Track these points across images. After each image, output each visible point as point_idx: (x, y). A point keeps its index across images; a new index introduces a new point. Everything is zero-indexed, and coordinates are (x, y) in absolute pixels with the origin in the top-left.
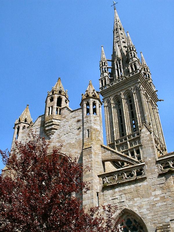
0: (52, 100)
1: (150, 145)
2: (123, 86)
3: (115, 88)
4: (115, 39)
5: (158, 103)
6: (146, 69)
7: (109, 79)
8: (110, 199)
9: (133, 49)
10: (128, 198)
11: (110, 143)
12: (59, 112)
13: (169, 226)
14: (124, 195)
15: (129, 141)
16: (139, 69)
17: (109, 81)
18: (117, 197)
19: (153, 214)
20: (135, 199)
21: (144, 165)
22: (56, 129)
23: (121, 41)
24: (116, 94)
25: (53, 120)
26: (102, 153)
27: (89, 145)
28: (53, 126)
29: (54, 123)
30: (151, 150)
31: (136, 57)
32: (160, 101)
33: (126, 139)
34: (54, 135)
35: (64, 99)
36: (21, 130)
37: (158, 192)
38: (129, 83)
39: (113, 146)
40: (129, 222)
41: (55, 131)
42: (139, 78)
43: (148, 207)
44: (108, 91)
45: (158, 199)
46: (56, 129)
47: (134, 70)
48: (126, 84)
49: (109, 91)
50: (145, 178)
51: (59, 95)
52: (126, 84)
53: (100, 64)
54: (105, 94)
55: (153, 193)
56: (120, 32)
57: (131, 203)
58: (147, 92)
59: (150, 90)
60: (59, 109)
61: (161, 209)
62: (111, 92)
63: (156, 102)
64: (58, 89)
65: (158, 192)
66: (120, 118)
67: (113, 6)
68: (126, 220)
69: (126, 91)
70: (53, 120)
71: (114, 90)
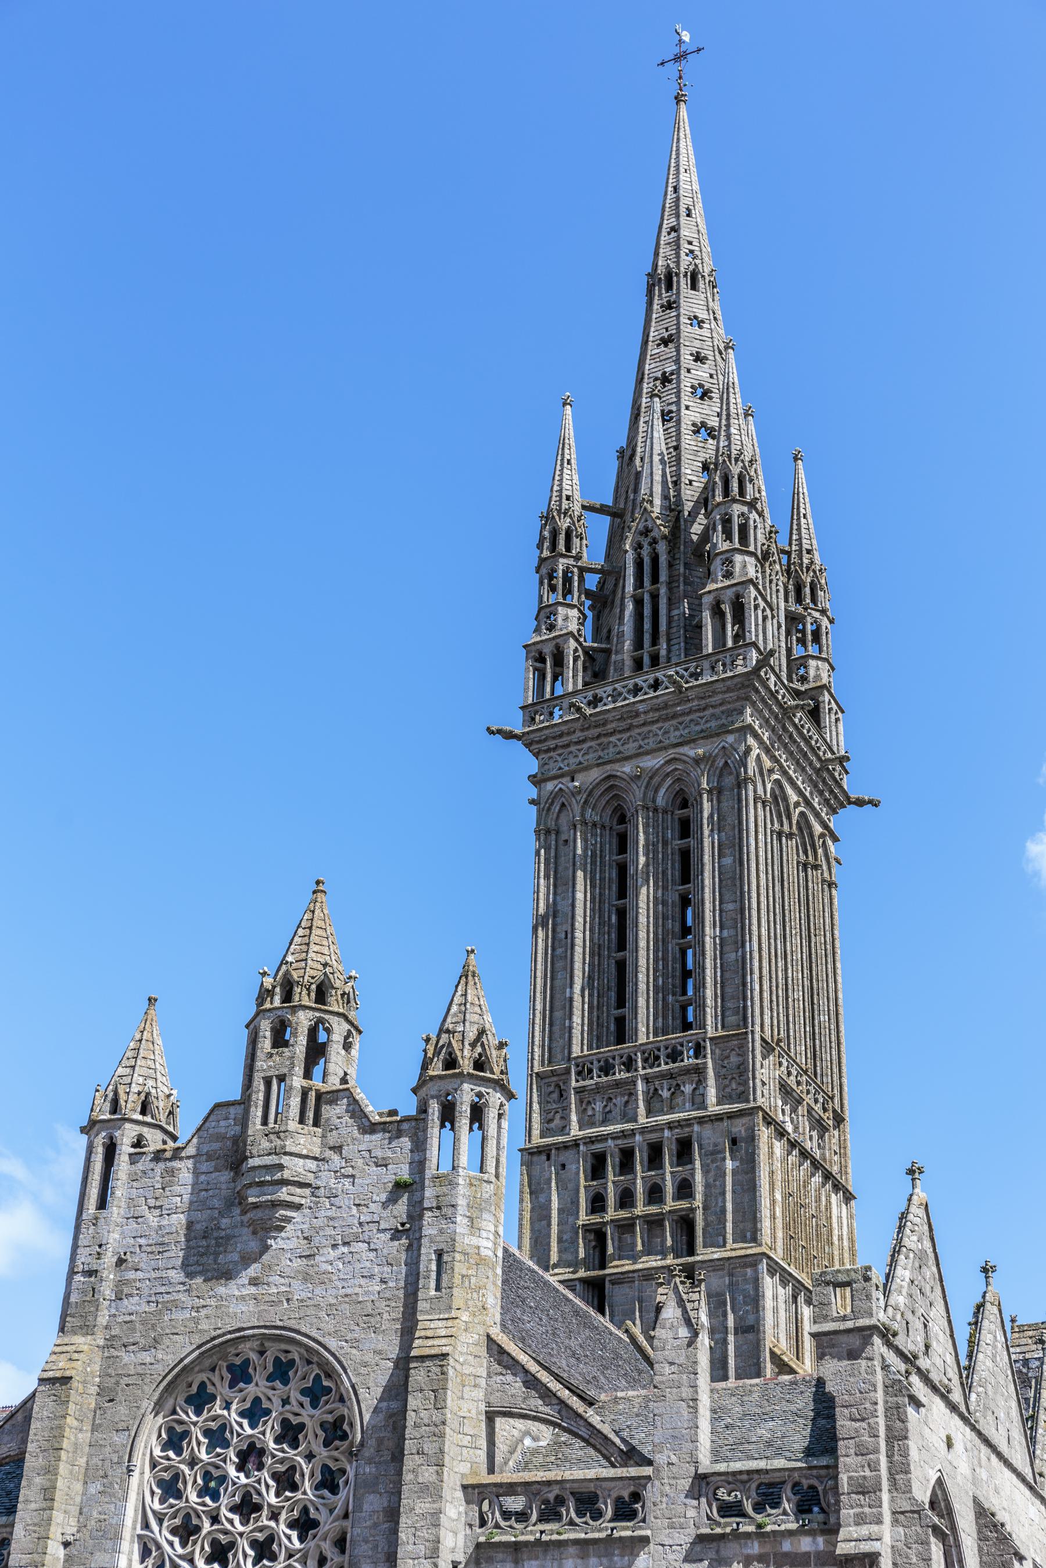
0: (280, 1041)
1: (686, 1392)
2: (654, 727)
3: (610, 727)
4: (652, 349)
5: (842, 821)
6: (808, 590)
7: (580, 652)
9: (742, 492)
11: (537, 1140)
12: (310, 1114)
15: (647, 1079)
16: (754, 644)
17: (580, 663)
21: (649, 1478)
22: (298, 1207)
23: (686, 384)
24: (608, 767)
25: (285, 1160)
26: (489, 1376)
27: (436, 1342)
28: (283, 1194)
29: (286, 1174)
30: (685, 1412)
31: (752, 549)
32: (860, 803)
33: (629, 1064)
34: (283, 1234)
35: (340, 1028)
36: (122, 1165)
38: (689, 713)
39: (558, 1086)
41: (289, 1213)
42: (747, 698)
44: (565, 740)
46: (298, 1207)
47: (730, 643)
48: (674, 716)
49: (574, 738)
50: (645, 1541)
51: (317, 1014)
52: (674, 722)
53: (542, 539)
54: (548, 750)
56: (692, 302)
58: (785, 773)
59: (805, 755)
60: (312, 1096)
62: (585, 746)
63: (834, 811)
64: (313, 972)
66: (614, 918)
67: (672, 69)
69: (668, 762)
70: (285, 1160)
71: (599, 736)
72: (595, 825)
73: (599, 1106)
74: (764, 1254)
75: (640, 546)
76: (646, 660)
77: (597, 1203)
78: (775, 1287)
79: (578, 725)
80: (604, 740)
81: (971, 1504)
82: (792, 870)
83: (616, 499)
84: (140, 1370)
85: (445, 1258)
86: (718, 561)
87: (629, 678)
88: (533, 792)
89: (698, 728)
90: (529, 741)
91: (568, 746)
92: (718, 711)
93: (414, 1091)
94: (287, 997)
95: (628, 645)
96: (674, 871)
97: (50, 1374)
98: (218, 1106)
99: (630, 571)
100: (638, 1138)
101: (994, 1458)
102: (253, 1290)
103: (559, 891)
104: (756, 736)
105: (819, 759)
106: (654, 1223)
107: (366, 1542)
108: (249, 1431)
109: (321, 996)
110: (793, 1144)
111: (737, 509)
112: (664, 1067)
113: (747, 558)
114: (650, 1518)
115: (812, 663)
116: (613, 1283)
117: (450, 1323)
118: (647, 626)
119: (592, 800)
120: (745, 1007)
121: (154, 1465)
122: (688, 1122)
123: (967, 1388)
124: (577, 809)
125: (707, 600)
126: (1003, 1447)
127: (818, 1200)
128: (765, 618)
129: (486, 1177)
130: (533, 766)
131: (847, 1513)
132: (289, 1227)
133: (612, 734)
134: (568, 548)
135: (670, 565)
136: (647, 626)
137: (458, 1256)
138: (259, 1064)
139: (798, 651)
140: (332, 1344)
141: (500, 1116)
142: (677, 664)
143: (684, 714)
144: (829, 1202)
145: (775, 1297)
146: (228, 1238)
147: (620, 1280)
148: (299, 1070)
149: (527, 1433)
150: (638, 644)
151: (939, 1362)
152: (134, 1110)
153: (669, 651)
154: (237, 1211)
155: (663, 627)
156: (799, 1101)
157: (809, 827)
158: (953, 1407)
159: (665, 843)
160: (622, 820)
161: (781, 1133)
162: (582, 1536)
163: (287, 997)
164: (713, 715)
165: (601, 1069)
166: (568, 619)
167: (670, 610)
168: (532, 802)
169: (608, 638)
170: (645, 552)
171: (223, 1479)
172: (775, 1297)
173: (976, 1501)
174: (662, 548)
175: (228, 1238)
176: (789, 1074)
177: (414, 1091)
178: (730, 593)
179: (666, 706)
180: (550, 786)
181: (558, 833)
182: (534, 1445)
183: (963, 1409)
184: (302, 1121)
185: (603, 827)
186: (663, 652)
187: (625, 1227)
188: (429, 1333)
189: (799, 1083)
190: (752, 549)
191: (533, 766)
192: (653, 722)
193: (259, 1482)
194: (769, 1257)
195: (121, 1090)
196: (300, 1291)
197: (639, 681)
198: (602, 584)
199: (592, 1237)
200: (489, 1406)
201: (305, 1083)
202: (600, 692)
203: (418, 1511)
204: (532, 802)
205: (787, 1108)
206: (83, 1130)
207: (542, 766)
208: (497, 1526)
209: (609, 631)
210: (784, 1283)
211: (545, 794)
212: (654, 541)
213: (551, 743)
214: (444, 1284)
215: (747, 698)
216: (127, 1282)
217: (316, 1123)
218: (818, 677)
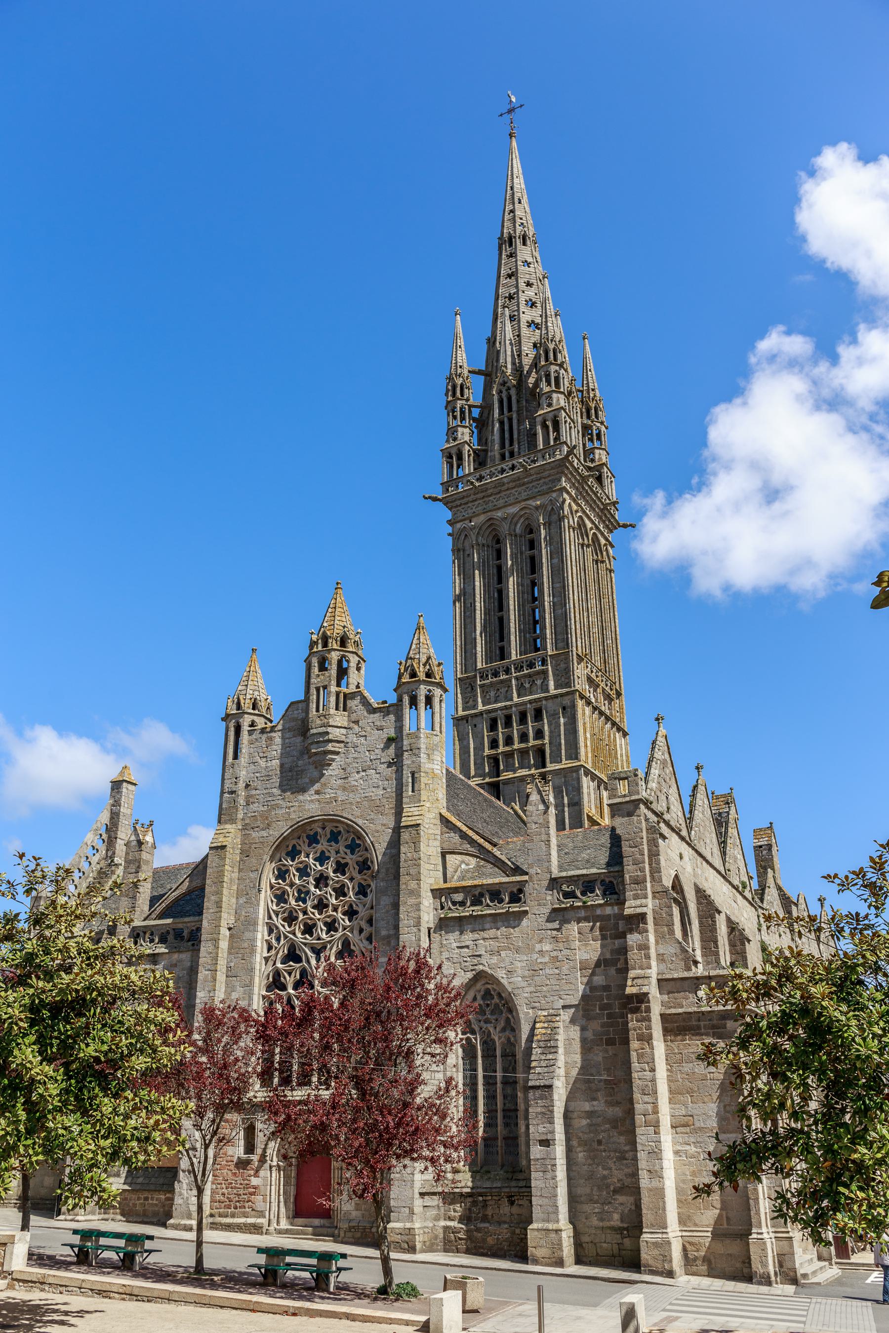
0: (323, 668)
1: (544, 837)
3: (489, 492)
4: (503, 281)
6: (593, 411)
7: (471, 452)
8: (455, 945)
9: (555, 359)
10: (489, 949)
11: (461, 713)
12: (341, 705)
13: (558, 1018)
14: (481, 941)
15: (517, 678)
16: (565, 443)
17: (471, 458)
18: (467, 943)
19: (532, 989)
20: (503, 953)
21: (526, 881)
22: (337, 753)
23: (522, 298)
24: (489, 514)
25: (329, 729)
26: (442, 834)
27: (413, 818)
28: (330, 747)
29: (331, 737)
31: (562, 390)
33: (507, 671)
35: (354, 660)
36: (245, 737)
37: (547, 947)
40: (487, 994)
41: (333, 757)
42: (563, 472)
43: (526, 973)
44: (466, 500)
45: (546, 959)
46: (337, 753)
47: (552, 443)
48: (523, 484)
49: (470, 499)
50: (526, 913)
52: (524, 487)
53: (448, 390)
54: (457, 506)
55: (538, 947)
56: (524, 253)
57: (494, 960)
58: (584, 512)
60: (342, 696)
61: (548, 982)
62: (476, 503)
64: (338, 631)
65: (547, 947)
66: (496, 595)
67: (507, 117)
68: (482, 993)
69: (521, 509)
70: (329, 729)
71: (483, 498)
72: (483, 545)
73: (492, 694)
74: (582, 766)
75: (501, 392)
76: (507, 454)
77: (494, 744)
78: (588, 782)
79: (472, 492)
80: (486, 499)
81: (693, 886)
82: (590, 564)
83: (487, 366)
84: (261, 840)
85: (416, 775)
86: (544, 397)
87: (499, 464)
88: (450, 529)
89: (537, 490)
90: (446, 502)
91: (467, 503)
92: (546, 480)
93: (395, 690)
94: (325, 645)
95: (497, 447)
96: (527, 568)
97: (215, 845)
98: (292, 703)
99: (496, 406)
100: (514, 709)
101: (704, 863)
102: (317, 797)
103: (466, 581)
104: (568, 493)
105: (602, 503)
106: (524, 753)
107: (383, 920)
108: (320, 868)
109: (343, 641)
110: (595, 709)
111: (553, 368)
112: (526, 672)
113: (559, 395)
114: (528, 901)
115: (597, 451)
116: (504, 784)
117: (420, 808)
118: (507, 435)
119: (482, 532)
120: (567, 638)
121: (272, 887)
122: (539, 700)
123: (689, 829)
124: (474, 537)
125: (539, 420)
126: (709, 858)
127: (609, 736)
128: (570, 428)
129: (435, 733)
130: (449, 515)
131: (629, 894)
132: (334, 764)
133: (490, 496)
134: (462, 395)
135: (518, 401)
136: (507, 435)
137: (422, 774)
138: (312, 680)
139: (589, 445)
140: (360, 822)
141: (441, 701)
142: (524, 456)
143: (529, 483)
144: (615, 737)
145: (589, 787)
146: (302, 771)
147: (508, 782)
148: (334, 682)
149: (463, 862)
150: (503, 446)
151: (674, 816)
152: (249, 708)
153: (519, 449)
154: (306, 757)
155: (515, 436)
156: (598, 686)
157: (598, 540)
158: (682, 839)
159: (521, 553)
160: (498, 542)
161: (589, 703)
162: (494, 912)
163: (325, 645)
164: (544, 483)
165: (493, 674)
166: (464, 434)
167: (519, 426)
168: (450, 535)
169: (486, 443)
170: (504, 395)
171: (308, 892)
172: (589, 787)
173: (696, 885)
174: (513, 392)
175: (302, 771)
176: (592, 672)
177: (395, 690)
178: (551, 415)
179: (519, 479)
180: (458, 525)
181: (464, 550)
182: (467, 867)
183: (688, 839)
184: (337, 709)
185: (488, 546)
186: (516, 450)
187: (509, 755)
188: (410, 814)
189: (597, 676)
190: (562, 390)
191: (449, 515)
192: (513, 488)
193: (326, 893)
194: (584, 767)
195: (241, 697)
196: (341, 796)
197: (504, 466)
198: (481, 414)
199: (492, 761)
200: (442, 848)
201: (338, 689)
202: (483, 473)
203: (409, 903)
204: (450, 535)
205: (592, 690)
206: (223, 719)
207: (454, 515)
208: (450, 909)
209: (487, 440)
210: (593, 780)
211: (456, 530)
212: (509, 389)
213: (458, 503)
214: (416, 789)
215: (563, 472)
216: (252, 796)
217: (345, 710)
218: (600, 459)
